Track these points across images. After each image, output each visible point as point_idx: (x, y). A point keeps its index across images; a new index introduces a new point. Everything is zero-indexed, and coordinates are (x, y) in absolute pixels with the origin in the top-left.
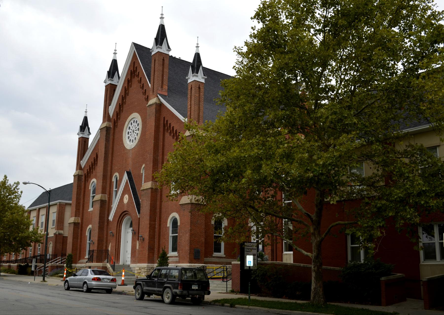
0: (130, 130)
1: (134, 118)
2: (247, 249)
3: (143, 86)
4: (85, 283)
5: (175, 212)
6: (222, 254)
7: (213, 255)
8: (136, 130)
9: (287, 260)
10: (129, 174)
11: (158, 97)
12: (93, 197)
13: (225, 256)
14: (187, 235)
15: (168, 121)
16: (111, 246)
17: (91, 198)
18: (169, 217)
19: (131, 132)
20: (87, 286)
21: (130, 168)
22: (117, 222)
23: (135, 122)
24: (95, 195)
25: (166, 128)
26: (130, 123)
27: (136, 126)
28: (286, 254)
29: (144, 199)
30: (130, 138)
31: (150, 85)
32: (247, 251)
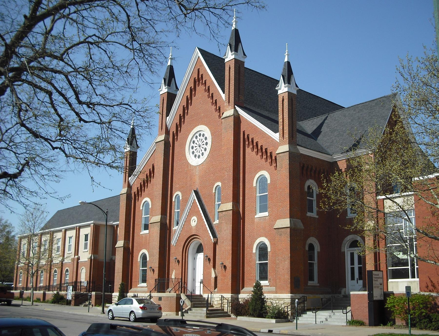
0: (195, 144)
1: (200, 131)
2: (375, 278)
3: (212, 96)
4: (132, 312)
5: (263, 236)
6: (315, 282)
7: (309, 284)
8: (204, 144)
9: (393, 288)
10: (196, 193)
11: (235, 108)
12: (219, 205)
13: (318, 285)
14: (286, 263)
15: (250, 135)
16: (175, 274)
17: (217, 207)
18: (254, 242)
19: (196, 147)
20: (135, 316)
21: (197, 186)
22: (182, 247)
23: (202, 136)
24: (220, 203)
25: (247, 143)
26: (195, 137)
27: (204, 140)
28: (392, 282)
29: (223, 222)
30: (195, 153)
31: (223, 96)
32: (375, 281)
